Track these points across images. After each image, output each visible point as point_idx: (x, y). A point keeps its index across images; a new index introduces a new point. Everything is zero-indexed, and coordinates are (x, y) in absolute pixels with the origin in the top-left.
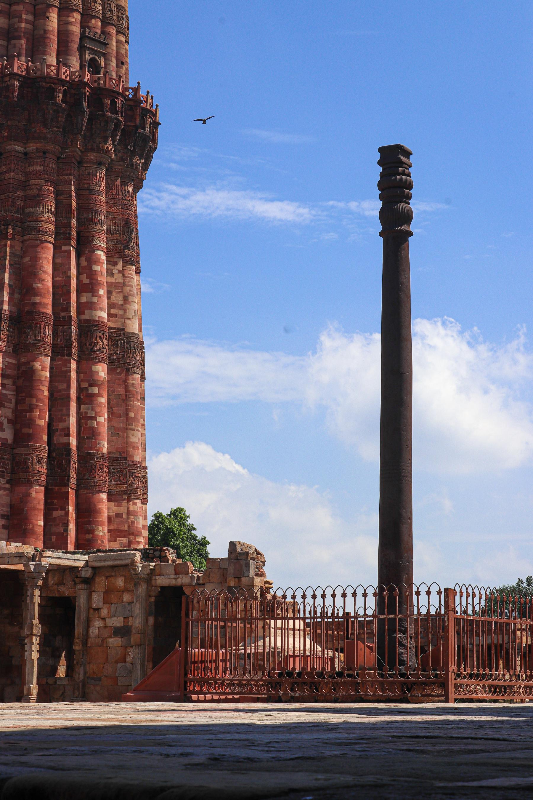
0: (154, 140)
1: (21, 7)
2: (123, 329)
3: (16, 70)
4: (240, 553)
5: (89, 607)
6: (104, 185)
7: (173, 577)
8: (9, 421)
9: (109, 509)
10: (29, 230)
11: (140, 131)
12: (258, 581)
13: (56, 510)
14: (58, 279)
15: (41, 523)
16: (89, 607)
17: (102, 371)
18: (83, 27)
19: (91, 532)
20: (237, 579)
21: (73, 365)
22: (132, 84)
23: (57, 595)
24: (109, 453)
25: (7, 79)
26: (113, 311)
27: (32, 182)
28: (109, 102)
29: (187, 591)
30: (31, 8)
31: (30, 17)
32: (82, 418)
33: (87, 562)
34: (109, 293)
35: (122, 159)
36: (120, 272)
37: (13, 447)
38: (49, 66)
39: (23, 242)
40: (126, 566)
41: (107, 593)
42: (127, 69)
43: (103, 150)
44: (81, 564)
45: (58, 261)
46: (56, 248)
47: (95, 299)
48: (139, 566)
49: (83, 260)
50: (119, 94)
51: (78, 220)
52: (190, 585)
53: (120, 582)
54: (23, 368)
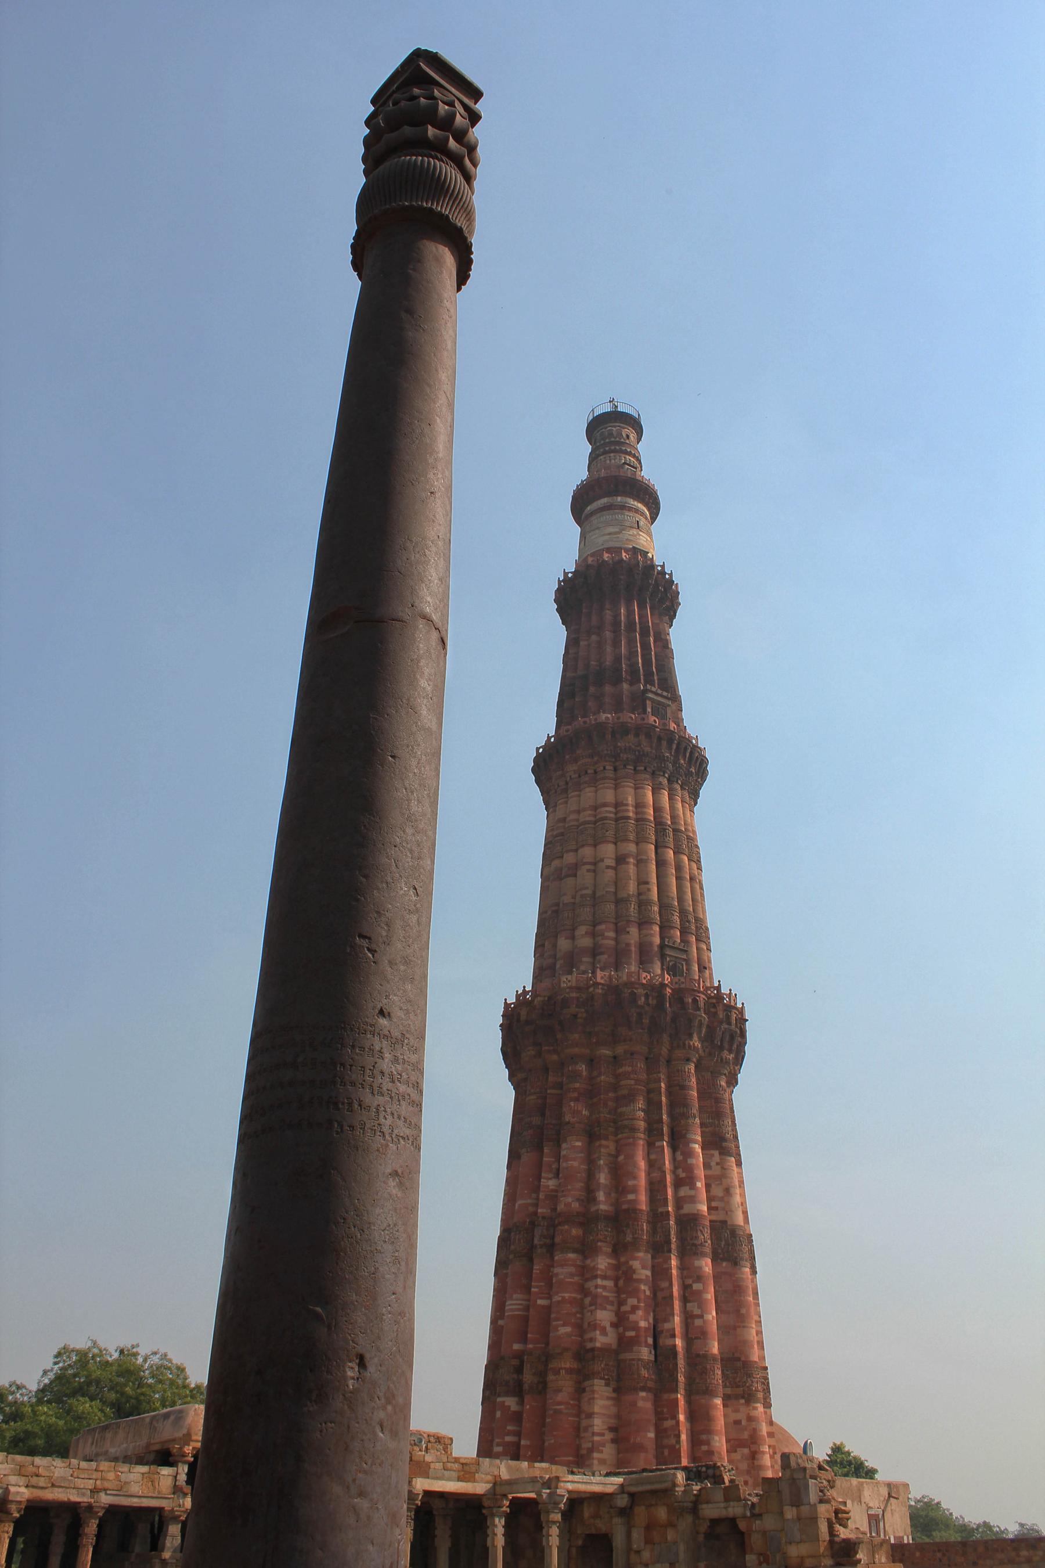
0: (743, 1034)
1: (603, 927)
2: (726, 1222)
3: (599, 980)
4: (794, 1470)
5: (629, 1549)
6: (694, 1080)
7: (722, 1505)
8: (614, 1325)
9: (725, 1416)
10: (621, 1127)
11: (725, 1026)
12: (822, 1509)
13: (667, 1419)
14: (654, 1175)
15: (651, 1435)
16: (629, 1549)
17: (706, 1265)
18: (662, 938)
19: (708, 1443)
20: (794, 1509)
21: (674, 1262)
22: (716, 984)
23: (593, 1531)
24: (721, 1353)
25: (591, 989)
26: (714, 1204)
27: (623, 1083)
28: (690, 1000)
29: (742, 1525)
30: (612, 926)
31: (612, 934)
32: (688, 1318)
33: (622, 1485)
34: (708, 1186)
35: (710, 1054)
36: (717, 1164)
37: (617, 1352)
38: (630, 974)
39: (617, 1142)
40: (665, 1491)
41: (649, 1528)
42: (711, 974)
43: (690, 1046)
44: (610, 1489)
45: (653, 1157)
46: (650, 1145)
47: (692, 1193)
48: (680, 1489)
49: (678, 1153)
50: (699, 992)
51: (671, 1115)
52: (744, 1517)
53: (662, 1513)
54: (624, 1268)
